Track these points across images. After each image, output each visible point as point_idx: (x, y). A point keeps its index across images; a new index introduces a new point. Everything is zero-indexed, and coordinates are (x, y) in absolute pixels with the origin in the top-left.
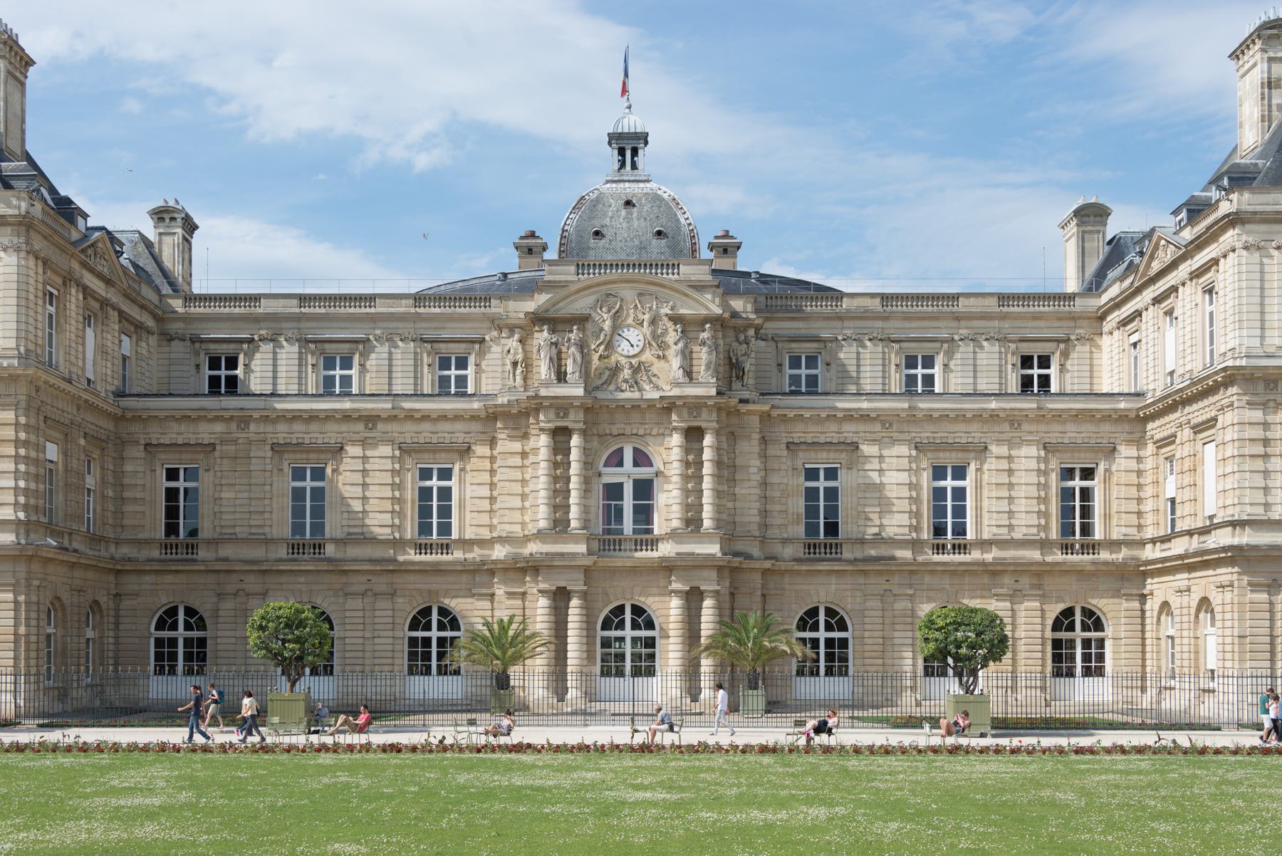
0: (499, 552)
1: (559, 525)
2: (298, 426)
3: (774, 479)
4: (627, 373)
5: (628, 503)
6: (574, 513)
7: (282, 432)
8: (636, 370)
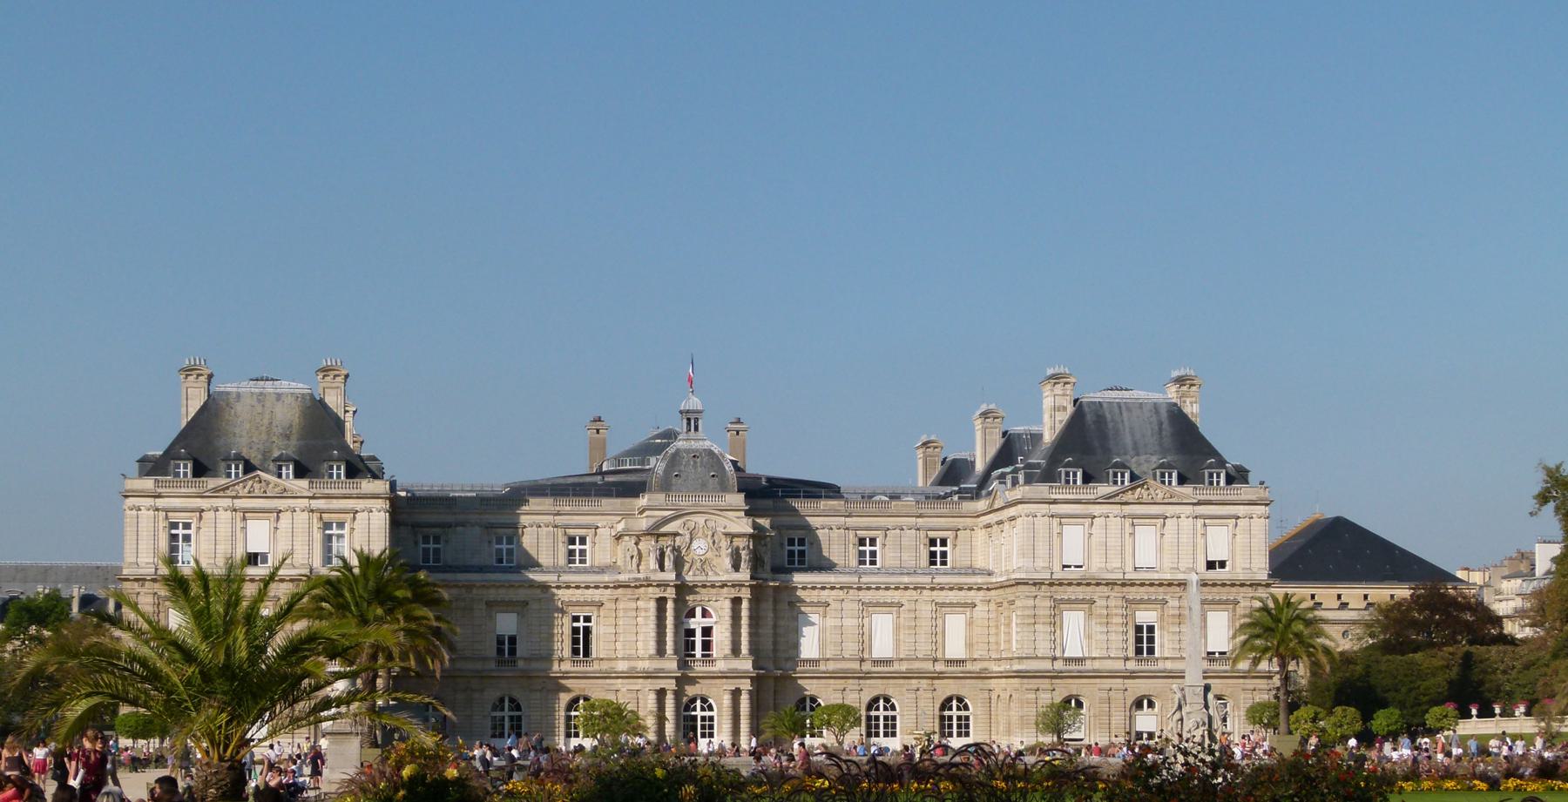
0: (622, 666)
1: (661, 651)
2: (502, 591)
3: (782, 623)
5: (698, 639)
7: (492, 594)
8: (703, 563)
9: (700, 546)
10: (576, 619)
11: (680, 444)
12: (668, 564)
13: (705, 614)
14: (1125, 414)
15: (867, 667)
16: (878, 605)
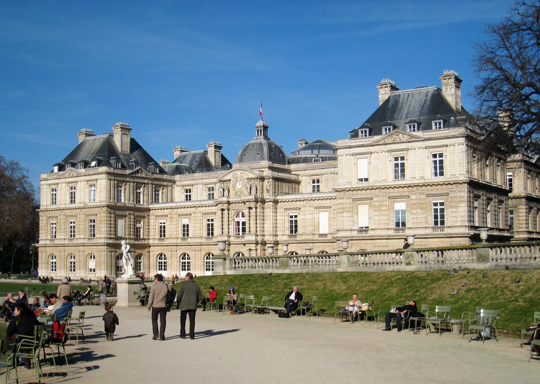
4: (239, 193)
5: (241, 227)
6: (226, 231)
9: (239, 186)
10: (209, 220)
11: (252, 142)
12: (226, 193)
13: (243, 216)
14: (410, 98)
15: (316, 237)
16: (320, 208)
